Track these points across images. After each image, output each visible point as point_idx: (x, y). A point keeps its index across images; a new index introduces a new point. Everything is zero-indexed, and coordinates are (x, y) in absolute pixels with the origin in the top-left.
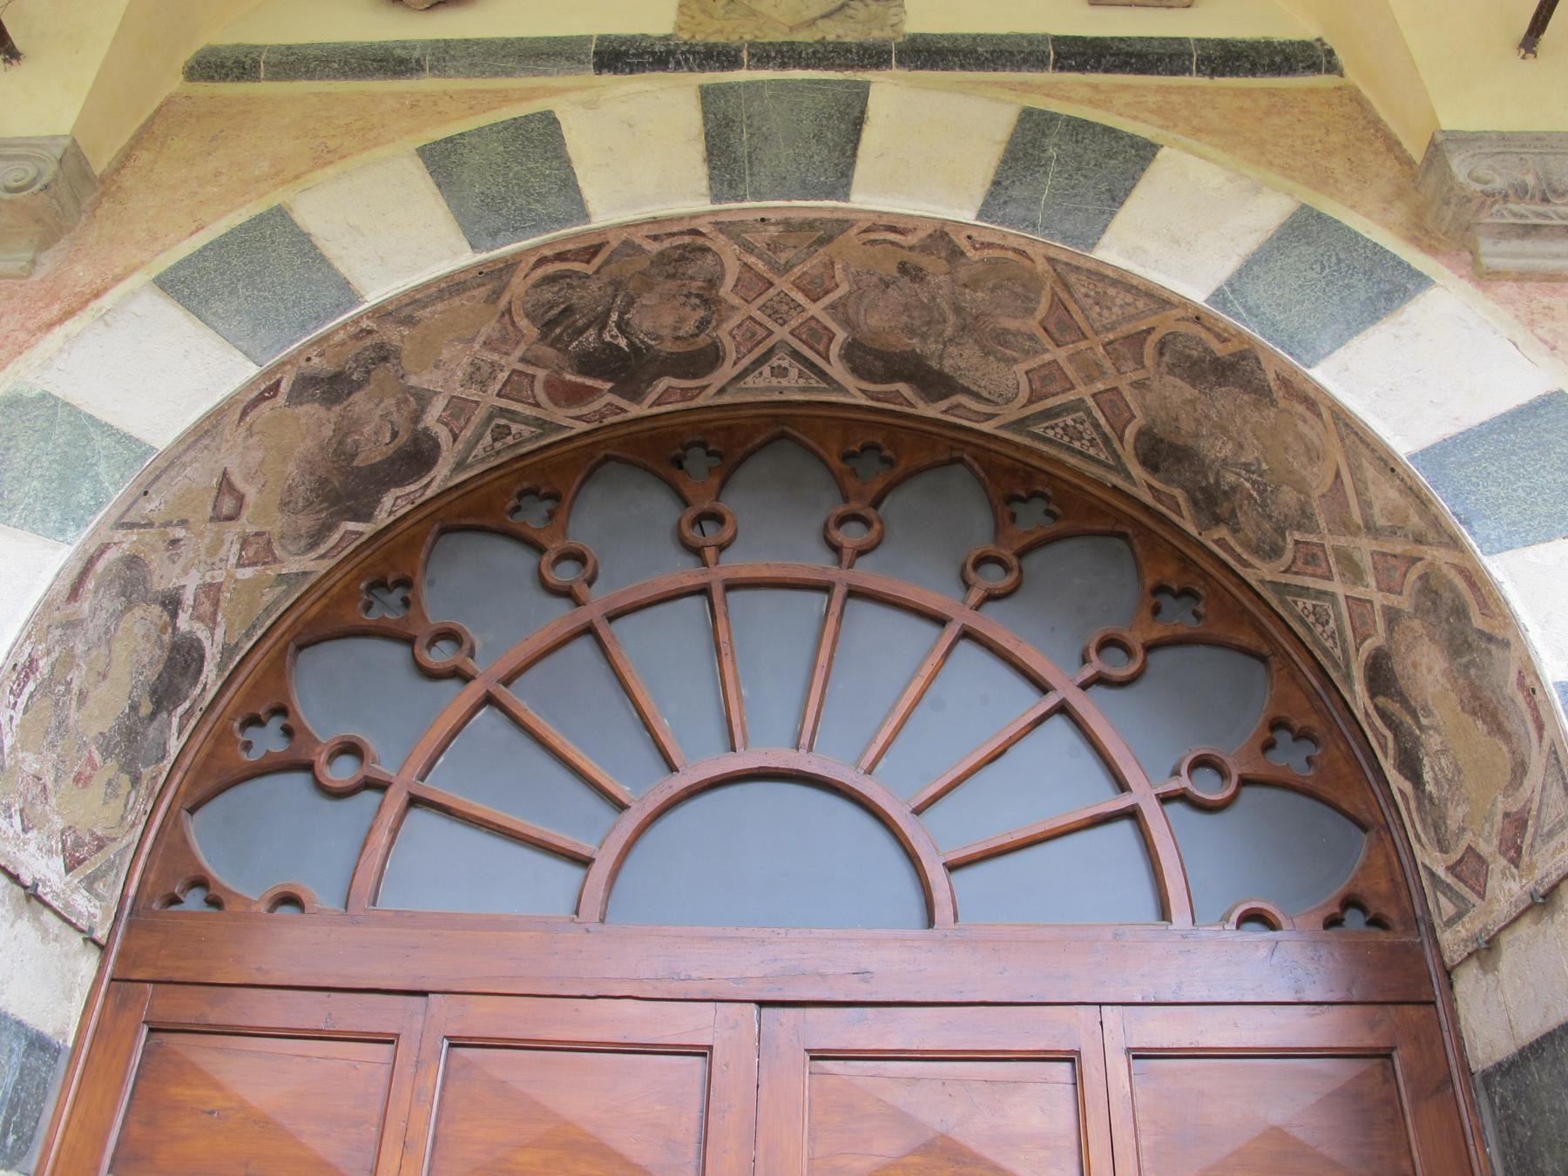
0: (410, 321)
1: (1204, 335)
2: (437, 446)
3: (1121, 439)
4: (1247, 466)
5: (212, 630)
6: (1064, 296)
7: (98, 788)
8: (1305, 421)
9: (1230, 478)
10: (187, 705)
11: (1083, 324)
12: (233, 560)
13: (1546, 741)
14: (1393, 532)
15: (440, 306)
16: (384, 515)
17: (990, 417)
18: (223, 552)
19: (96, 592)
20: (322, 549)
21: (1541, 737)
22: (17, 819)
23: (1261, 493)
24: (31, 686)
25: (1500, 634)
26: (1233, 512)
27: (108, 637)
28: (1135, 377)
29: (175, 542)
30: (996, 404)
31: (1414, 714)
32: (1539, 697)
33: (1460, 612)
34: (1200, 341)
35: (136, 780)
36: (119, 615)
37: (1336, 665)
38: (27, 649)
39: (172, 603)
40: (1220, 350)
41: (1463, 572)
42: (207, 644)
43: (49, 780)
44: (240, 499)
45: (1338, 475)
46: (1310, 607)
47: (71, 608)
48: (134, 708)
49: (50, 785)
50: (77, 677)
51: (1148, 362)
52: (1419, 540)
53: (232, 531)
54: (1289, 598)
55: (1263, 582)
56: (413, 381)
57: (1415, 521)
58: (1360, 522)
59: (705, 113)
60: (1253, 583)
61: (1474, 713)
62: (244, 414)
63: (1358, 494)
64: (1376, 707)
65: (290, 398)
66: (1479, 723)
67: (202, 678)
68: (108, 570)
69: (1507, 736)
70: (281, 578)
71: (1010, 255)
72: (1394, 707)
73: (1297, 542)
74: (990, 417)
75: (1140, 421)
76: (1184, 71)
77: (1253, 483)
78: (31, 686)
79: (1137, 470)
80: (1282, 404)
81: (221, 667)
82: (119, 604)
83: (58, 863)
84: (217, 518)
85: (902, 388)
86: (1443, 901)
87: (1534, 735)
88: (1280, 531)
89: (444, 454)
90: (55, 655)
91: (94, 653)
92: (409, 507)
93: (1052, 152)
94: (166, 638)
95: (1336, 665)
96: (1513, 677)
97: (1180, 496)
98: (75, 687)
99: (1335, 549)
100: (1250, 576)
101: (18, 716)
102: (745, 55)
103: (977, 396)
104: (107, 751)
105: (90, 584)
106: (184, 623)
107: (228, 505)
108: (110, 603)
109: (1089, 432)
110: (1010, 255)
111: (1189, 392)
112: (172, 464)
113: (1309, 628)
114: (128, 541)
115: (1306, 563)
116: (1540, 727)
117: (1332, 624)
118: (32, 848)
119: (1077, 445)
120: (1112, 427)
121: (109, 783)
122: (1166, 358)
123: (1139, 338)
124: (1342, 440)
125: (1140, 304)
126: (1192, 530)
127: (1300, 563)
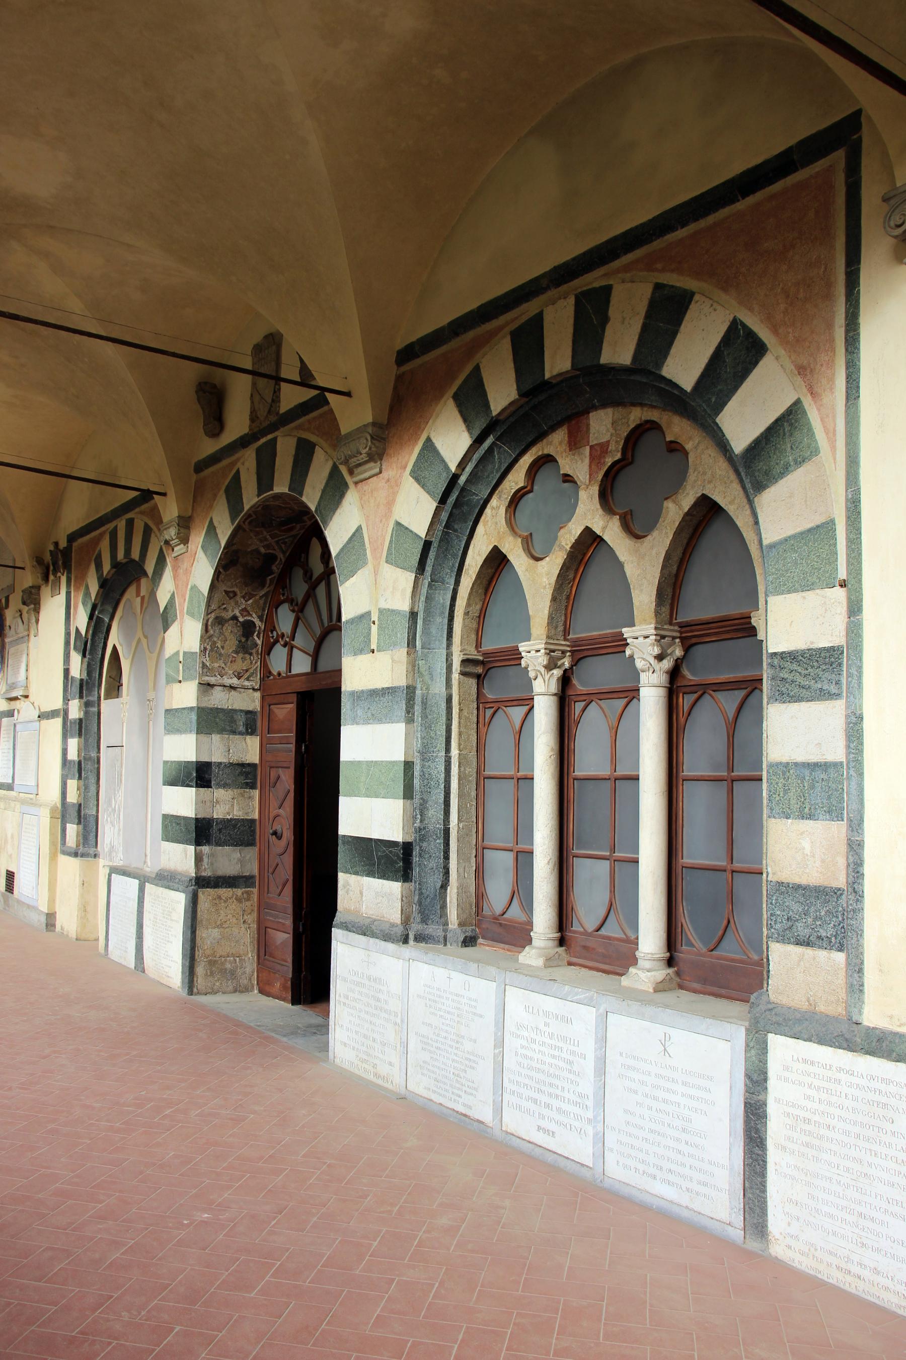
0: (233, 545)
2: (272, 554)
5: (251, 615)
7: (239, 660)
10: (257, 633)
12: (244, 602)
15: (236, 539)
16: (276, 571)
18: (239, 602)
19: (212, 628)
20: (267, 585)
22: (219, 676)
24: (208, 652)
27: (221, 633)
29: (225, 608)
35: (251, 654)
36: (222, 628)
38: (202, 646)
39: (235, 618)
42: (252, 619)
43: (223, 665)
44: (234, 591)
47: (208, 634)
48: (240, 641)
49: (224, 667)
50: (219, 645)
53: (238, 598)
56: (249, 550)
62: (218, 580)
65: (225, 571)
67: (257, 625)
68: (212, 623)
70: (261, 597)
78: (208, 652)
81: (261, 620)
82: (220, 626)
83: (236, 679)
84: (231, 598)
89: (277, 554)
90: (210, 644)
91: (220, 638)
92: (282, 566)
94: (239, 624)
98: (219, 646)
101: (208, 659)
104: (237, 652)
105: (210, 627)
106: (241, 619)
107: (231, 595)
108: (217, 629)
112: (210, 598)
114: (213, 616)
118: (226, 679)
121: (242, 658)
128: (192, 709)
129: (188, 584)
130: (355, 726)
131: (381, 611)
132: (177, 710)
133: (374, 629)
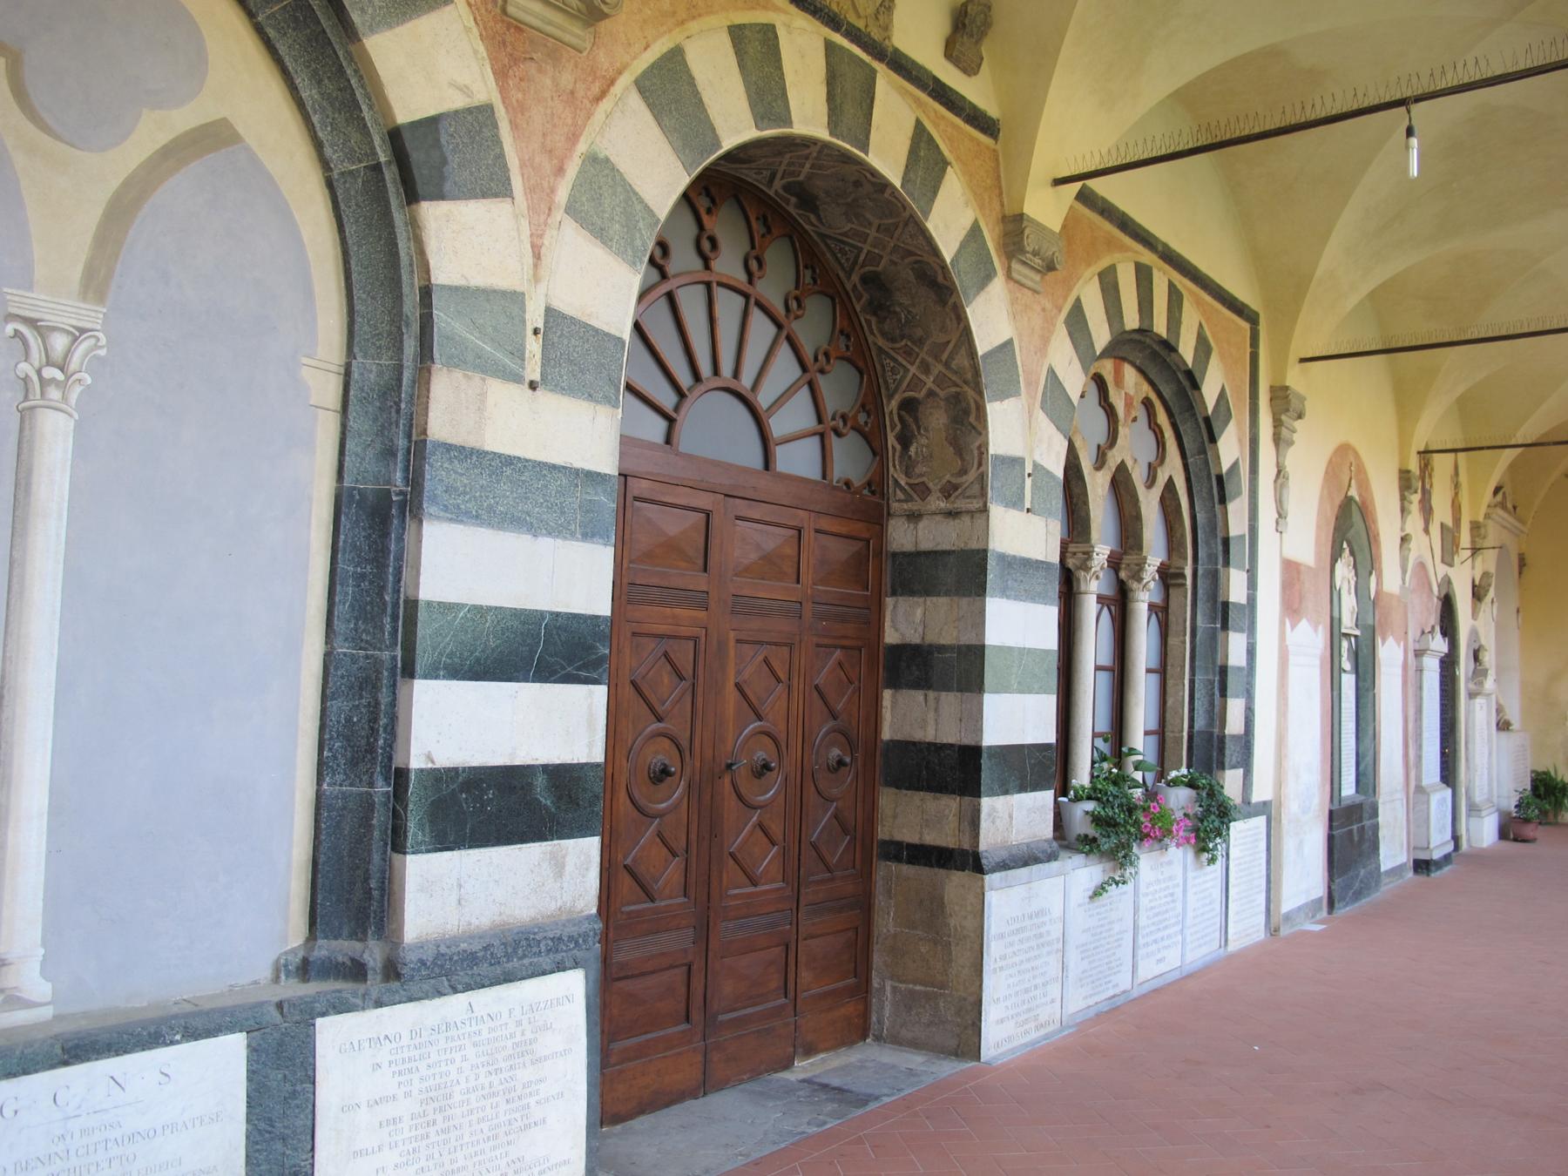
1: (940, 272)
3: (862, 267)
4: (909, 312)
6: (901, 225)
8: (951, 320)
9: (898, 309)
11: (896, 235)
13: (981, 470)
14: (956, 373)
17: (814, 225)
21: (978, 468)
23: (906, 322)
25: (979, 428)
26: (885, 318)
28: (894, 259)
30: (822, 223)
31: (919, 428)
32: (985, 456)
33: (967, 412)
34: (936, 272)
37: (887, 388)
40: (940, 279)
41: (976, 402)
45: (949, 342)
46: (892, 364)
51: (906, 261)
52: (966, 382)
54: (883, 356)
55: (875, 344)
57: (969, 376)
58: (944, 360)
59: (827, 63)
60: (870, 342)
61: (951, 444)
63: (951, 352)
64: (899, 414)
66: (951, 449)
69: (963, 460)
71: (899, 205)
72: (910, 420)
73: (906, 345)
74: (814, 225)
75: (880, 269)
76: (958, 115)
77: (906, 316)
79: (855, 278)
80: (947, 310)
85: (793, 200)
86: (898, 492)
87: (975, 465)
88: (902, 337)
93: (922, 154)
95: (887, 388)
96: (977, 444)
97: (866, 297)
99: (923, 359)
100: (870, 339)
102: (844, 28)
103: (819, 218)
109: (852, 257)
110: (899, 205)
111: (912, 278)
113: (884, 370)
115: (905, 352)
116: (980, 464)
117: (898, 377)
119: (839, 255)
120: (864, 260)
122: (916, 266)
123: (911, 253)
124: (961, 336)
125: (926, 248)
126: (858, 309)
127: (901, 351)
128: (592, 477)
129: (573, 138)
130: (1005, 600)
131: (1036, 465)
132: (509, 461)
133: (1028, 482)
